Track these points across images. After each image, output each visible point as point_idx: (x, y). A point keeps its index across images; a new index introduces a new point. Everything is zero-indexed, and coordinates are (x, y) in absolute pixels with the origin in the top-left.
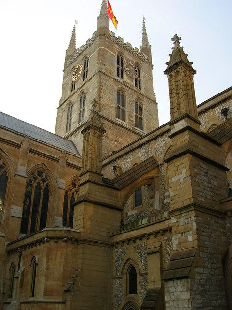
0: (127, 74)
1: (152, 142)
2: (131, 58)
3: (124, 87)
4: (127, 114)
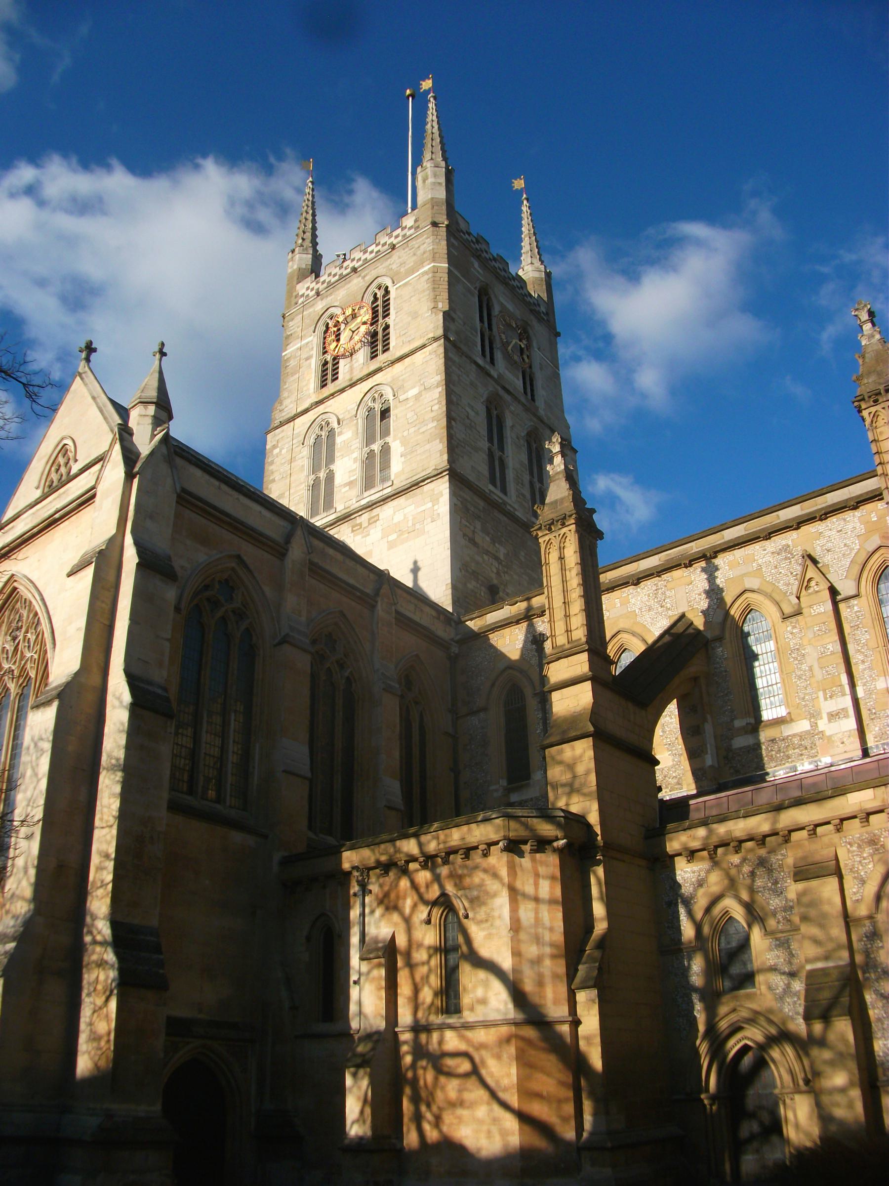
0: (507, 356)
1: (677, 573)
2: (510, 307)
3: (501, 392)
4: (510, 475)
